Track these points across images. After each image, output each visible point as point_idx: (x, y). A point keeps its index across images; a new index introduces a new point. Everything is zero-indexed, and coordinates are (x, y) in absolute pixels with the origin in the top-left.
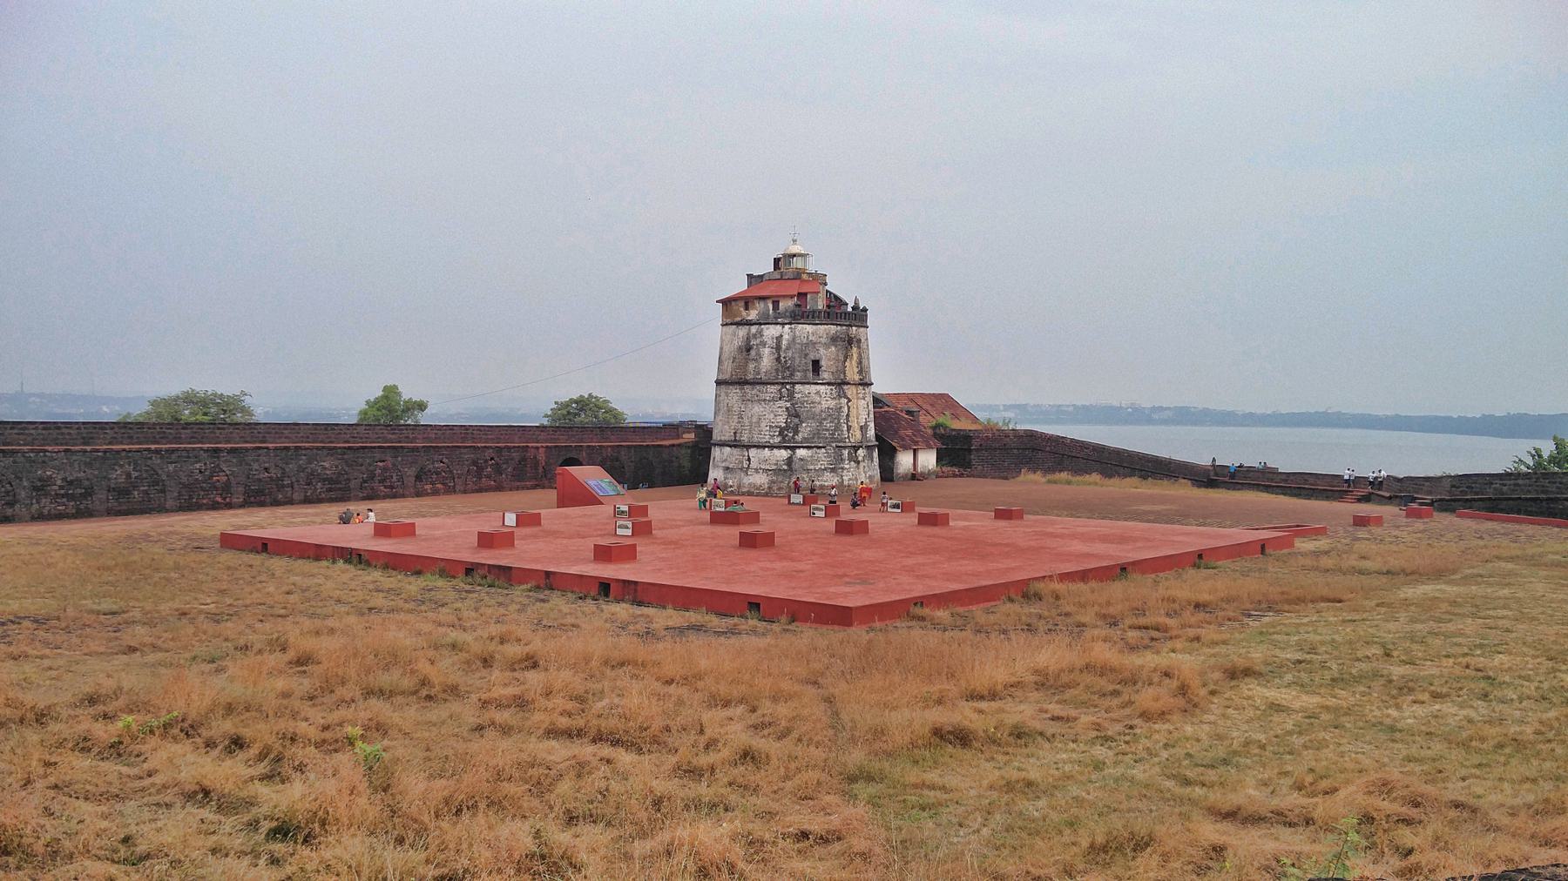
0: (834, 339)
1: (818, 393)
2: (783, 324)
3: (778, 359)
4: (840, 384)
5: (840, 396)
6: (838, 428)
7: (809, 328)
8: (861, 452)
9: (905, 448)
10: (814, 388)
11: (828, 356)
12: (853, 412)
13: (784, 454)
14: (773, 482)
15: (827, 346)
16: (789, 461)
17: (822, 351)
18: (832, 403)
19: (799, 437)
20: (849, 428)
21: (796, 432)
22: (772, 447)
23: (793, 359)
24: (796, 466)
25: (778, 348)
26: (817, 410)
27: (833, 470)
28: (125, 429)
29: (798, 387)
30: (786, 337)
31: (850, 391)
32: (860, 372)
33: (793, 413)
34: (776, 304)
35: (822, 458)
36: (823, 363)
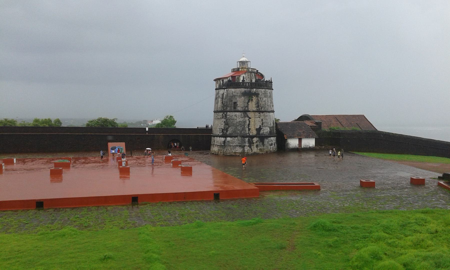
0: (244, 94)
1: (236, 115)
2: (224, 89)
3: (222, 103)
4: (245, 112)
5: (245, 117)
6: (244, 129)
7: (233, 90)
8: (255, 140)
9: (292, 137)
10: (234, 114)
11: (241, 102)
12: (252, 123)
13: (223, 139)
14: (219, 150)
15: (240, 97)
16: (224, 142)
17: (238, 99)
18: (241, 120)
19: (228, 133)
21: (227, 132)
22: (220, 137)
23: (227, 102)
24: (226, 144)
25: (222, 98)
26: (235, 122)
27: (240, 146)
28: (25, 129)
29: (228, 113)
30: (225, 94)
31: (250, 115)
32: (258, 106)
33: (226, 123)
34: (223, 81)
35: (236, 141)
36: (238, 103)
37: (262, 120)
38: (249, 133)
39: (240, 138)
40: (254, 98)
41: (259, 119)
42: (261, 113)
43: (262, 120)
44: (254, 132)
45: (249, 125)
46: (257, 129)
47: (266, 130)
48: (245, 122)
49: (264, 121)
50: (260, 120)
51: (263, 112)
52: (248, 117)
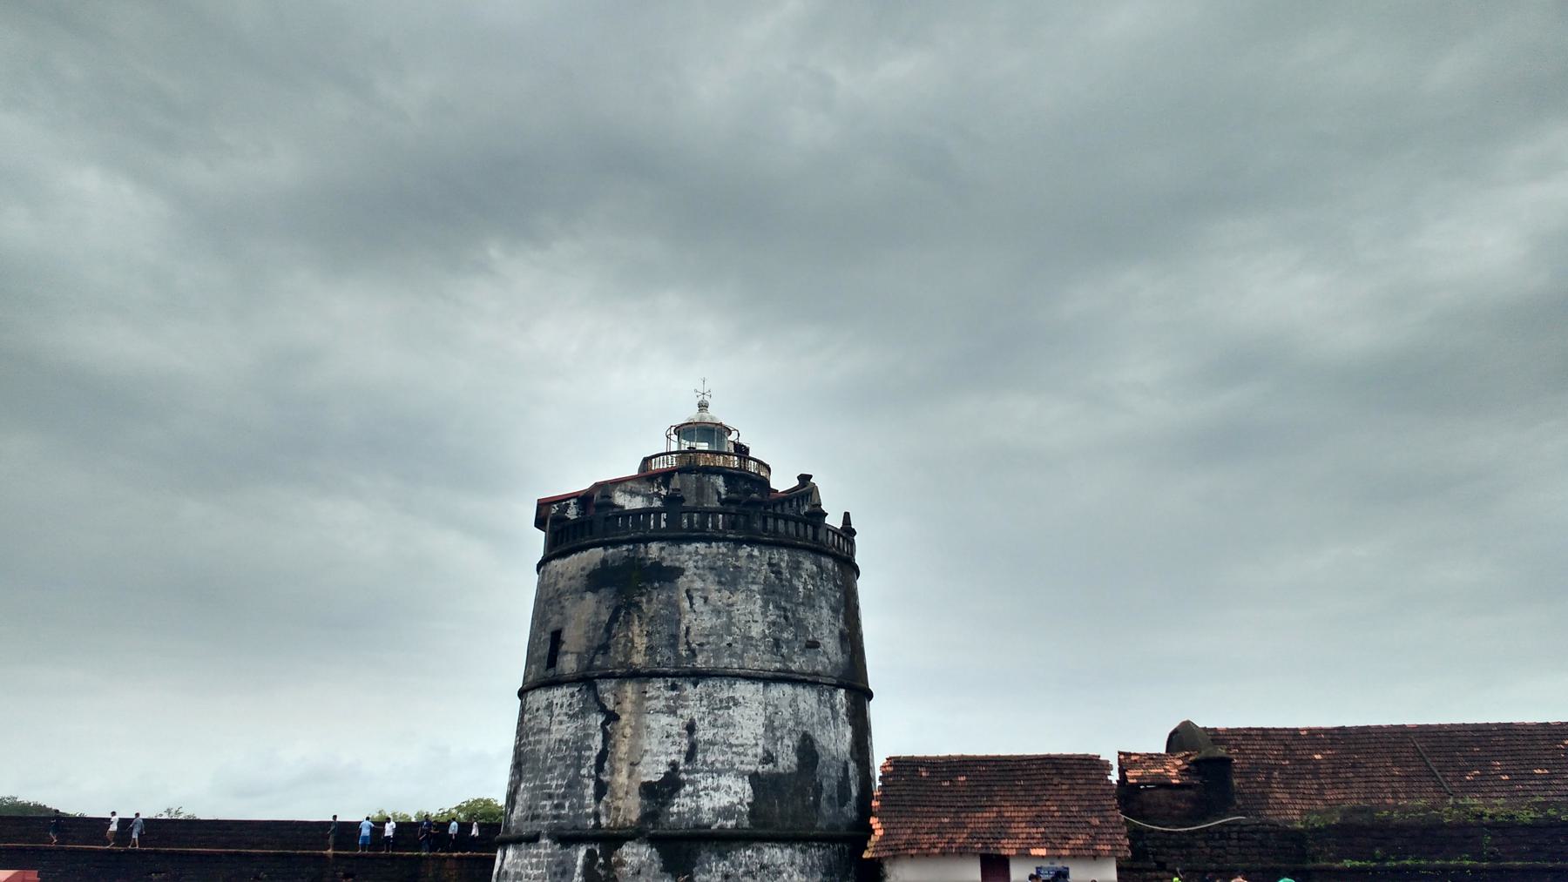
0: (597, 579)
5: (583, 713)
15: (579, 593)
20: (601, 789)
37: (691, 728)
38: (597, 815)
39: (546, 847)
40: (653, 602)
41: (665, 720)
42: (689, 688)
43: (691, 728)
44: (630, 808)
45: (602, 757)
46: (648, 790)
47: (720, 796)
48: (580, 745)
49: (704, 733)
50: (676, 725)
51: (698, 676)
52: (603, 709)
